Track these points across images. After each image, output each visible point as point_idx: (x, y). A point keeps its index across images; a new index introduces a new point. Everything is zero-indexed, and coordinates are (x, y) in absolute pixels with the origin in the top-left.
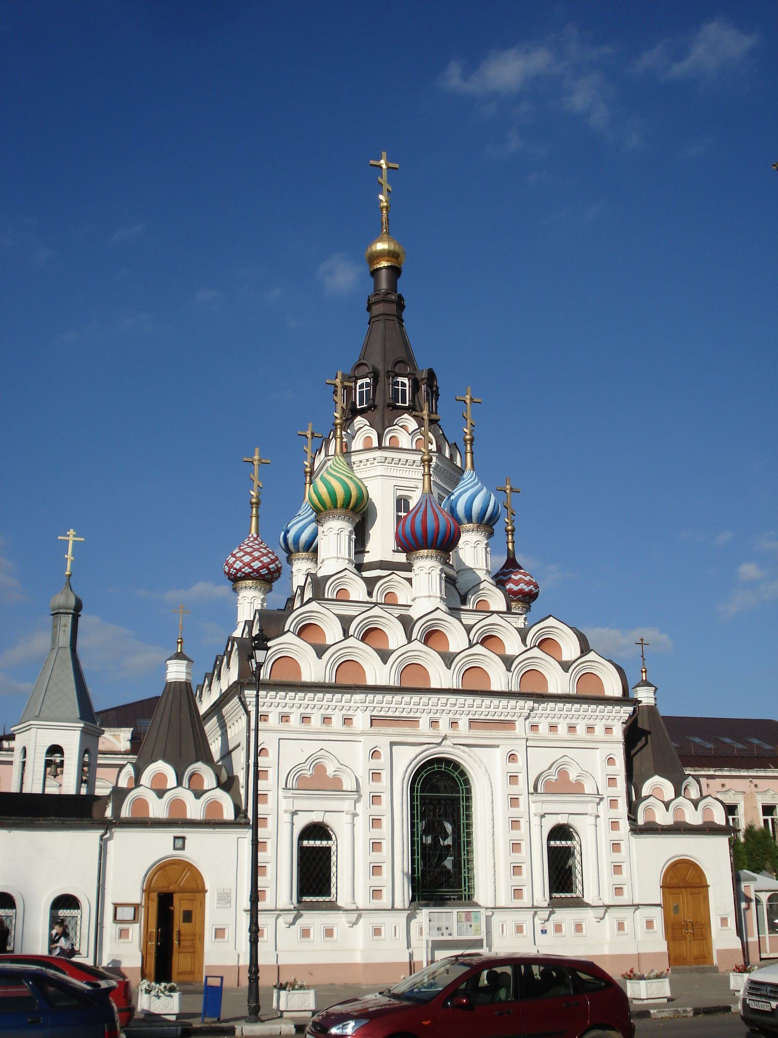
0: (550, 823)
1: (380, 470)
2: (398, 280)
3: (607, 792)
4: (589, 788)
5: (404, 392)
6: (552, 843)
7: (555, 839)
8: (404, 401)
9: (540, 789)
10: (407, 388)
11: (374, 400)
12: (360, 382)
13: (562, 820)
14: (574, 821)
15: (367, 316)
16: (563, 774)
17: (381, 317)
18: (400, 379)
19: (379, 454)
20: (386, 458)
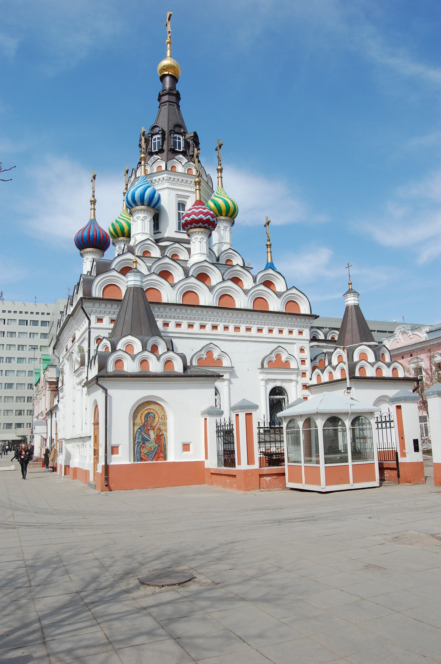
0: (271, 386)
1: (166, 185)
2: (176, 85)
3: (302, 368)
4: (293, 365)
5: (180, 143)
6: (272, 397)
7: (273, 395)
8: (180, 148)
9: (266, 366)
10: (181, 141)
11: (162, 146)
12: (154, 137)
13: (278, 384)
14: (285, 385)
15: (158, 103)
16: (278, 356)
17: (167, 103)
18: (177, 136)
19: (165, 176)
20: (170, 178)
